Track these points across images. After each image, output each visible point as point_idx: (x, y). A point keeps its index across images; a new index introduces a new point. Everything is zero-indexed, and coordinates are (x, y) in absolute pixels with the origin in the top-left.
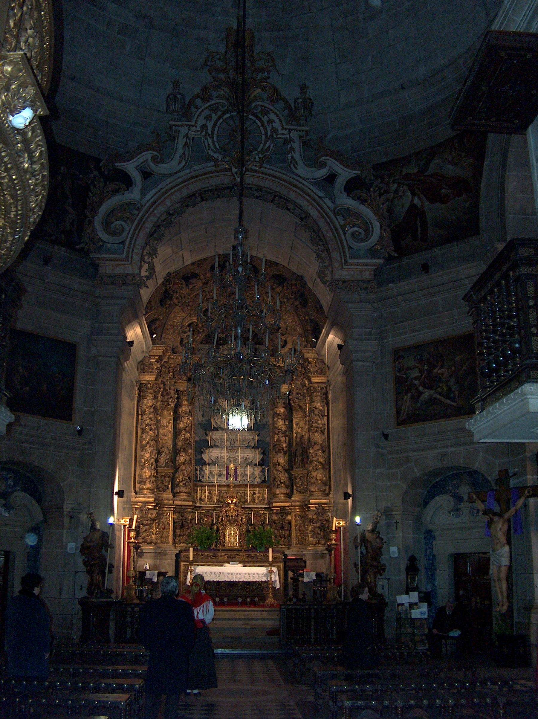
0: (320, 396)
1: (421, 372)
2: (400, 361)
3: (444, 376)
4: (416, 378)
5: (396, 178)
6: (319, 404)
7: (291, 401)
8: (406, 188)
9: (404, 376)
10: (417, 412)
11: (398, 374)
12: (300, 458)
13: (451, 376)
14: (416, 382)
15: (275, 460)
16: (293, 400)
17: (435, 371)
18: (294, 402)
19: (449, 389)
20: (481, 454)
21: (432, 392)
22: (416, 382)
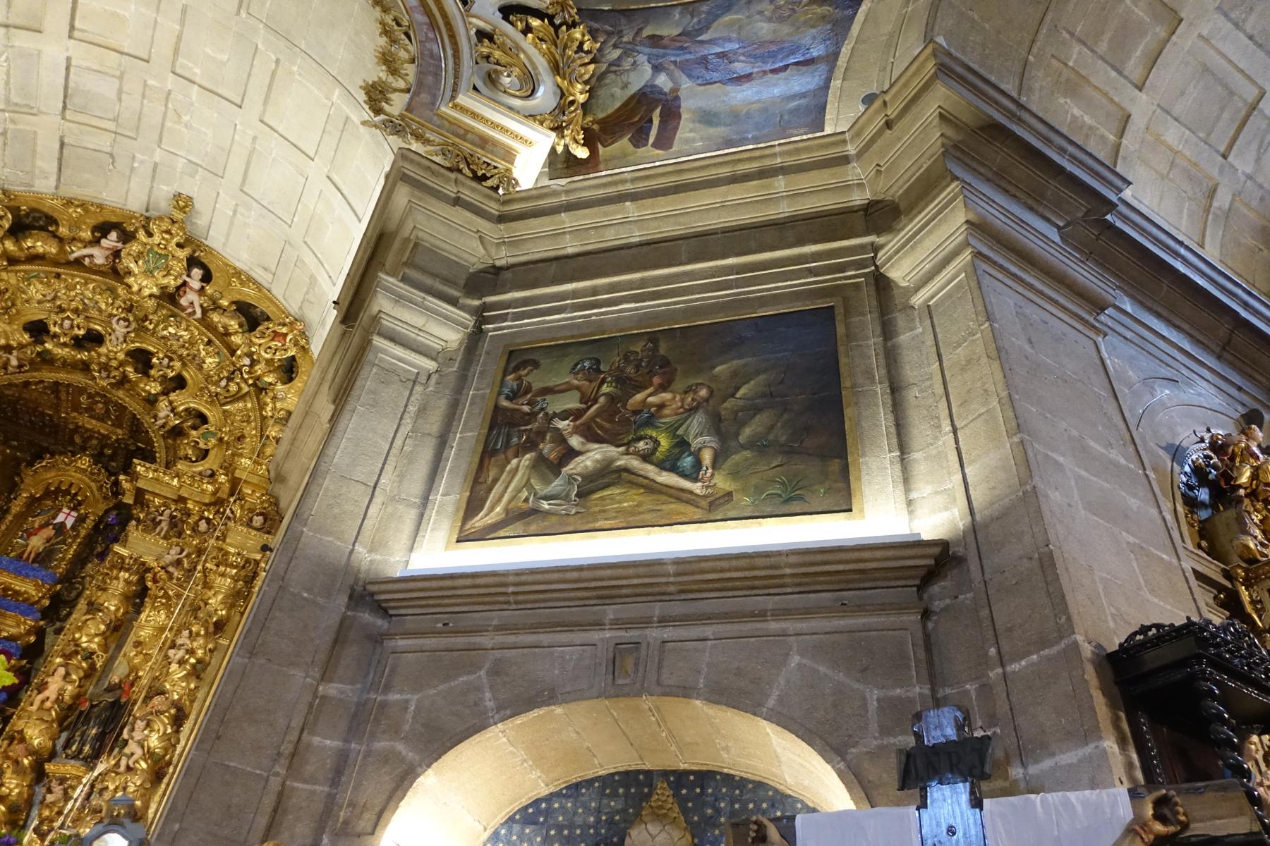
0: (232, 577)
1: (588, 400)
2: (523, 372)
3: (666, 411)
4: (564, 415)
5: (625, 39)
6: (220, 597)
7: (149, 576)
8: (642, 58)
9: (526, 408)
10: (545, 505)
11: (505, 403)
12: (94, 731)
13: (692, 410)
14: (562, 424)
15: (20, 725)
16: (155, 574)
17: (639, 397)
18: (155, 581)
19: (682, 445)
20: (795, 659)
21: (611, 451)
22: (562, 424)
